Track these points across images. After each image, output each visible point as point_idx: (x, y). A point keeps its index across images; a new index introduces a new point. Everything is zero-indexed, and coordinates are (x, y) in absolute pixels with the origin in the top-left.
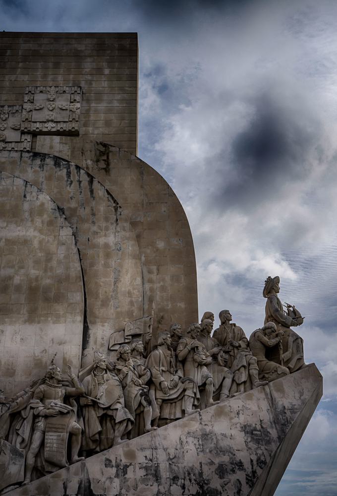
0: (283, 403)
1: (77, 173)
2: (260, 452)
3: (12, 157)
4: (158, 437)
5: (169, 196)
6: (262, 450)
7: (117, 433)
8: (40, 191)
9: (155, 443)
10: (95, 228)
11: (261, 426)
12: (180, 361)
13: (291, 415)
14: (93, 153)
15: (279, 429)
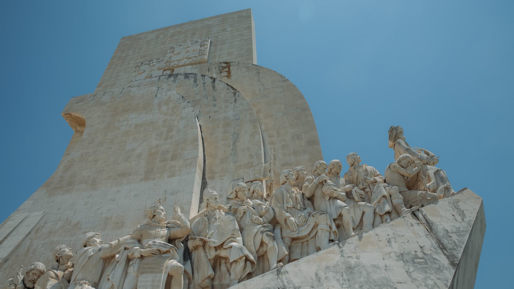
0: (444, 228)
1: (202, 79)
2: (430, 282)
3: (152, 81)
4: (287, 274)
5: (283, 82)
6: (433, 280)
7: (233, 276)
8: (169, 90)
9: (282, 281)
10: (216, 109)
11: (423, 253)
12: (308, 199)
13: (458, 239)
14: (218, 69)
15: (447, 254)
